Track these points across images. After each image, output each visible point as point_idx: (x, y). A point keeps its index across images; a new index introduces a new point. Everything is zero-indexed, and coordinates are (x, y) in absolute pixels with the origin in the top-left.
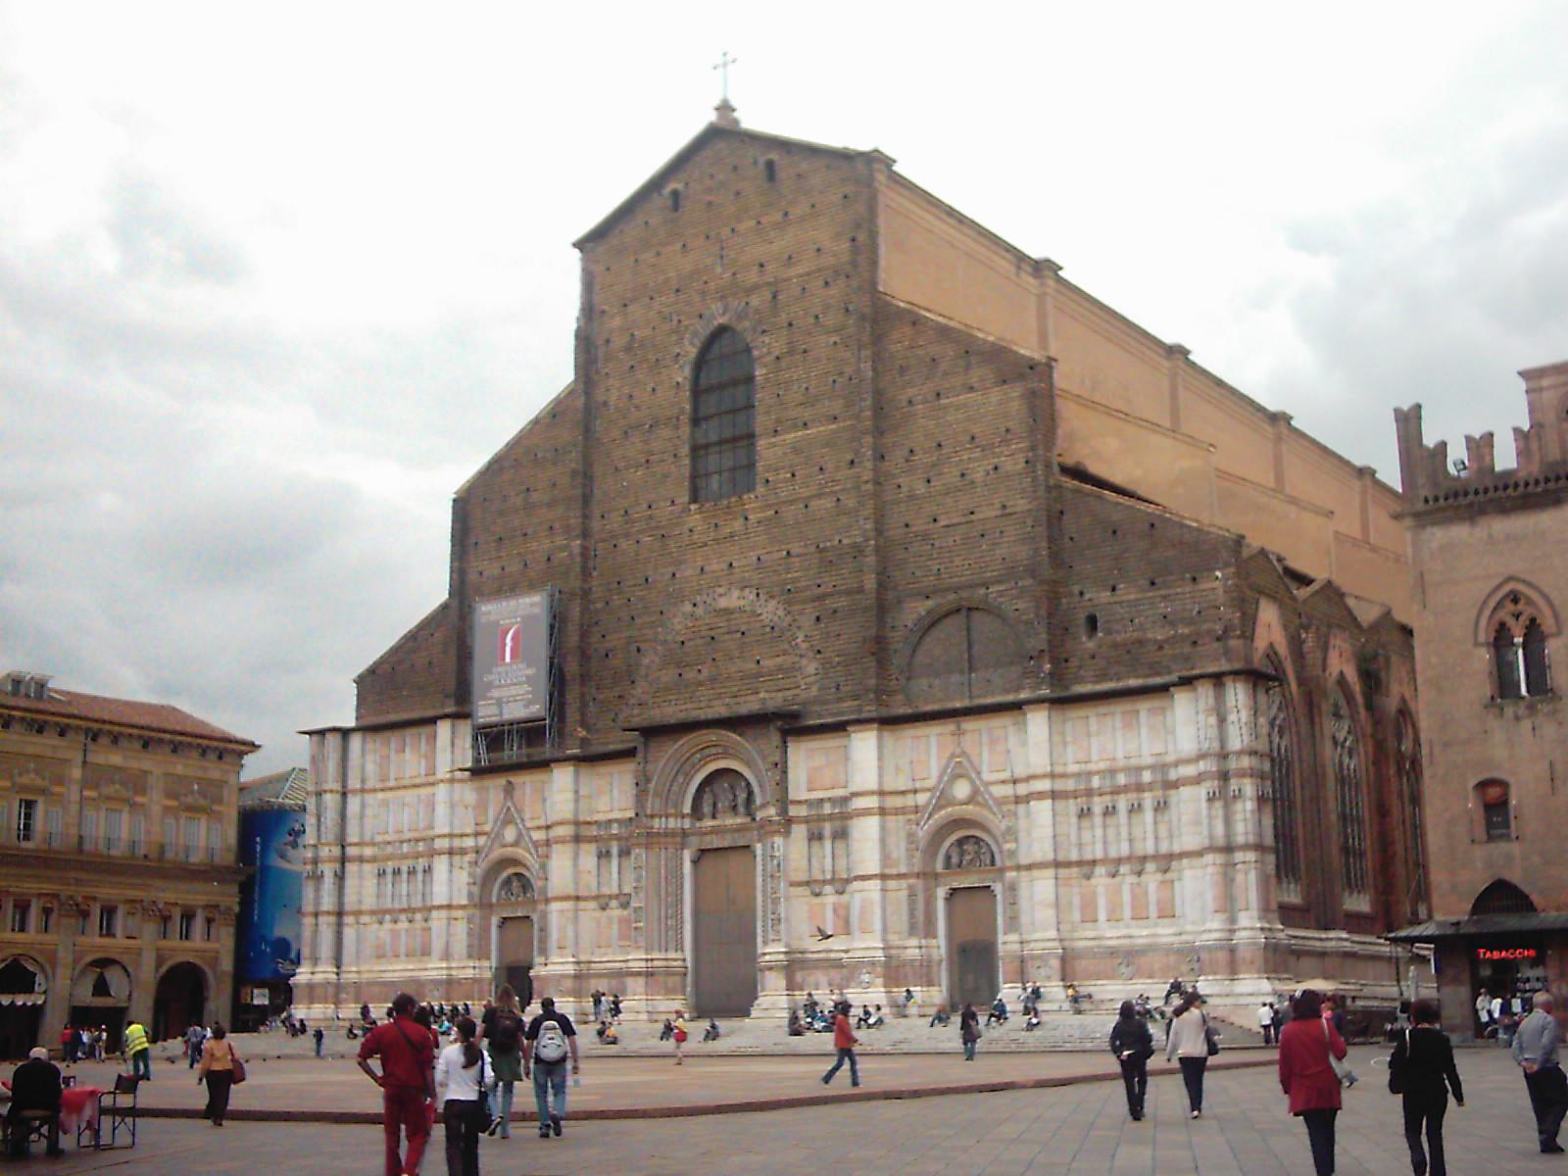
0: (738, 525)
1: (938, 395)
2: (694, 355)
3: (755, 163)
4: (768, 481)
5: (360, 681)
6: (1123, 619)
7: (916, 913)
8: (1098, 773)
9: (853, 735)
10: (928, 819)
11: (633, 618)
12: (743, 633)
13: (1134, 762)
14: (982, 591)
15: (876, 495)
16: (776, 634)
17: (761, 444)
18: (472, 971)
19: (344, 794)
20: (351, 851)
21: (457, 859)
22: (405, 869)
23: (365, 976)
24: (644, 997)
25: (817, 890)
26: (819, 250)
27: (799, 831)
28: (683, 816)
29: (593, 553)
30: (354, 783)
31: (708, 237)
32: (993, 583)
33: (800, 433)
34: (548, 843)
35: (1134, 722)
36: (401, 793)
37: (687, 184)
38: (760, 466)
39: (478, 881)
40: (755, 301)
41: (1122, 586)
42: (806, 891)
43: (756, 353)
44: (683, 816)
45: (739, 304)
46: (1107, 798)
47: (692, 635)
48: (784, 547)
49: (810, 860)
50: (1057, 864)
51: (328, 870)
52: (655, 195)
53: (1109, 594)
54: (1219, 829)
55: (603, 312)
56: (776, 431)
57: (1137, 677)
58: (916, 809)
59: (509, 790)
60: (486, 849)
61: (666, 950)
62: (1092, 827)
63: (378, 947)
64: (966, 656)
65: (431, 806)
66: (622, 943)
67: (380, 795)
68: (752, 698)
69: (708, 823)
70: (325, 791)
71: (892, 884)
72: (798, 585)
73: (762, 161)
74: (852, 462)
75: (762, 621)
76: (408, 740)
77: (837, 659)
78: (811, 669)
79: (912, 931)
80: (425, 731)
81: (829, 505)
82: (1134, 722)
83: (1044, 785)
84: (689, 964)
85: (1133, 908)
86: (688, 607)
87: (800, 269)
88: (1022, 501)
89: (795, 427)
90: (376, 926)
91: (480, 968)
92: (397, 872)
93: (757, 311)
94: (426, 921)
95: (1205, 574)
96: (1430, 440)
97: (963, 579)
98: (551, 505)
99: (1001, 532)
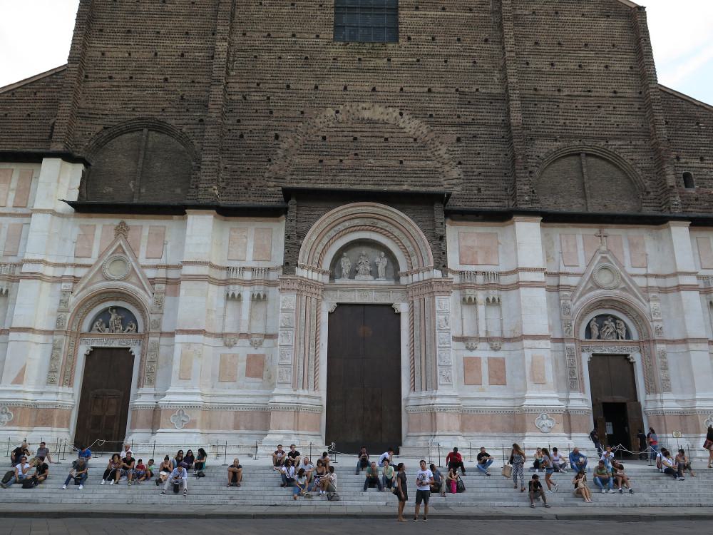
1: (557, 13)
4: (409, 38)
7: (576, 371)
9: (516, 223)
10: (579, 298)
11: (271, 113)
12: (386, 139)
14: (603, 143)
17: (403, 13)
24: (293, 432)
25: (474, 346)
27: (455, 296)
32: (610, 138)
33: (440, 13)
34: (177, 282)
38: (402, 27)
39: (72, 310)
41: (707, 158)
42: (461, 345)
44: (324, 273)
47: (335, 134)
48: (426, 85)
49: (462, 319)
53: (698, 161)
58: (568, 288)
59: (122, 230)
60: (86, 281)
61: (308, 388)
65: (17, 237)
72: (440, 113)
74: (486, 40)
77: (478, 170)
78: (456, 172)
80: (17, 169)
83: (691, 280)
84: (324, 403)
86: (330, 112)
88: (628, 91)
89: (436, 9)
91: (62, 393)
97: (586, 132)
98: (189, 16)
99: (614, 108)
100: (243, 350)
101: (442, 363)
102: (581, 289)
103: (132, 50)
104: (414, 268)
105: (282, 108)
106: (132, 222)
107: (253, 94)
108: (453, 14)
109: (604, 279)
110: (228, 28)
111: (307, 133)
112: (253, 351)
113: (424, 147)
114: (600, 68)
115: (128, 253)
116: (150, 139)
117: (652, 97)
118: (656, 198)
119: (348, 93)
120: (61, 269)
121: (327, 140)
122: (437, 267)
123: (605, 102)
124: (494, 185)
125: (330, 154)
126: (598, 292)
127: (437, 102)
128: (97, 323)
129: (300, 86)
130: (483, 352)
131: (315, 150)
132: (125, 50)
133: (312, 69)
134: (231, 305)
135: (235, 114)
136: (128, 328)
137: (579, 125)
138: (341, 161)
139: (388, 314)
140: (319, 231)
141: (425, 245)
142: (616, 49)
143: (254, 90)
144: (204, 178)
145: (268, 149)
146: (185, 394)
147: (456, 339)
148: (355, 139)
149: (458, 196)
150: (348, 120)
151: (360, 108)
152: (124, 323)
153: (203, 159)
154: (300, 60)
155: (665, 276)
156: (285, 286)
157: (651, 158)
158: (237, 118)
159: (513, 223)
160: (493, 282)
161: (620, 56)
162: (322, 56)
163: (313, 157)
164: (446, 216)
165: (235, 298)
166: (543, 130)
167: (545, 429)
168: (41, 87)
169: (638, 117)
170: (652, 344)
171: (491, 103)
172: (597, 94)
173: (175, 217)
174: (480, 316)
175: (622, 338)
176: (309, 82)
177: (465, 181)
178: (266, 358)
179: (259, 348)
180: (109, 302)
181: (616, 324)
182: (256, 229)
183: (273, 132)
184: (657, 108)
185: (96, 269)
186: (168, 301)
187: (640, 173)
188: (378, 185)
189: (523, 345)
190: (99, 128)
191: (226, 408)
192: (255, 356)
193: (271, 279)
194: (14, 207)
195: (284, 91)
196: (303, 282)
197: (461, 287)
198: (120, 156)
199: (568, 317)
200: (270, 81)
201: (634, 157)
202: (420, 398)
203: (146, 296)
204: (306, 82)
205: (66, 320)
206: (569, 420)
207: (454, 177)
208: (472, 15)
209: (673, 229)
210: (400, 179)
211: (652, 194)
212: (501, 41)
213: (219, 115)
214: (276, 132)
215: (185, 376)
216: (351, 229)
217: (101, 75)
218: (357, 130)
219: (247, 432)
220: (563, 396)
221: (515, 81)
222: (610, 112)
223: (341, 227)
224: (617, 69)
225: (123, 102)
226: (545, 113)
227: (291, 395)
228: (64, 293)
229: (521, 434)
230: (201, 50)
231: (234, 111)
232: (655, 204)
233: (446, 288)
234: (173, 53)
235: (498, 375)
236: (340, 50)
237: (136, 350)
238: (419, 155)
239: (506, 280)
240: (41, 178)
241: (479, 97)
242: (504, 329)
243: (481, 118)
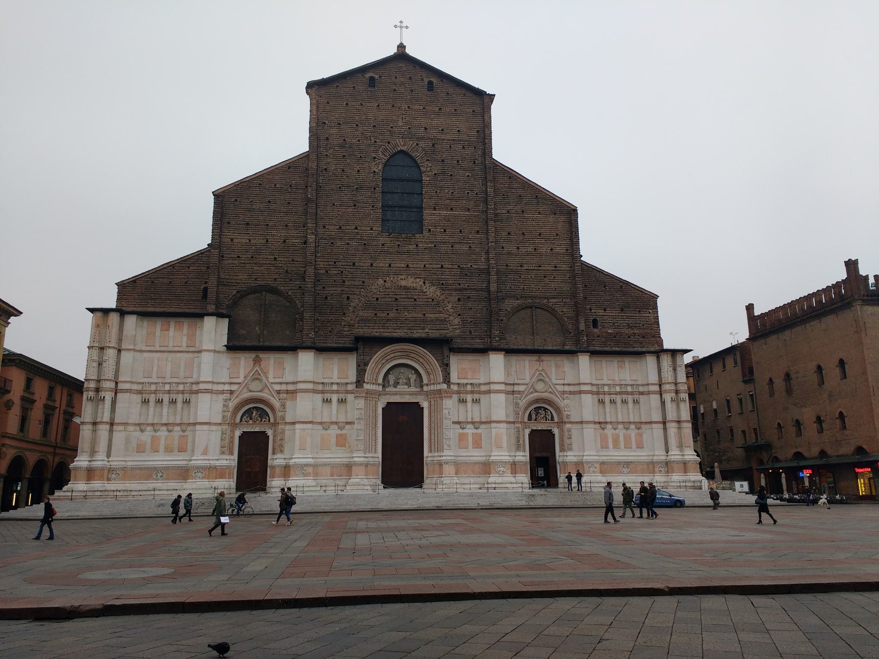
0: (412, 247)
1: (523, 212)
2: (383, 160)
3: (422, 79)
4: (430, 230)
5: (121, 285)
6: (610, 323)
7: (521, 440)
8: (607, 385)
10: (525, 397)
11: (344, 282)
12: (415, 300)
13: (623, 382)
14: (546, 301)
15: (495, 249)
16: (435, 304)
17: (426, 212)
18: (225, 462)
19: (119, 351)
20: (121, 386)
21: (214, 396)
22: (166, 398)
23: (129, 463)
26: (459, 131)
28: (379, 385)
29: (317, 245)
30: (124, 346)
31: (393, 106)
34: (294, 392)
35: (623, 366)
36: (165, 355)
37: (380, 77)
38: (425, 223)
39: (231, 410)
40: (422, 144)
41: (608, 309)
42: (458, 426)
43: (422, 169)
44: (379, 385)
45: (412, 145)
46: (614, 396)
50: (595, 423)
51: (108, 396)
52: (360, 75)
53: (603, 311)
54: (675, 414)
55: (325, 123)
56: (435, 208)
57: (618, 347)
58: (519, 392)
59: (257, 361)
62: (604, 408)
63: (139, 446)
64: (535, 328)
66: (339, 448)
67: (146, 355)
68: (421, 331)
69: (390, 389)
70: (109, 347)
71: (509, 426)
72: (448, 282)
73: (426, 80)
74: (478, 232)
75: (426, 295)
76: (172, 324)
79: (519, 447)
81: (466, 249)
82: (623, 366)
85: (625, 444)
86: (381, 281)
87: (448, 137)
88: (565, 266)
90: (138, 433)
92: (160, 402)
93: (423, 150)
94: (184, 431)
95: (645, 310)
96: (863, 272)
97: (537, 294)
99: (554, 277)
100: (334, 431)
101: (446, 438)
102: (526, 392)
103: (251, 237)
104: (432, 382)
105: (351, 279)
106: (262, 355)
107: (332, 269)
108: (458, 213)
109: (540, 386)
110: (315, 225)
111: (367, 296)
112: (339, 432)
113: (438, 304)
114: (548, 251)
115: (262, 375)
116: (267, 298)
117: (576, 272)
118: (574, 336)
119: (392, 269)
120: (222, 385)
121: (379, 300)
122: (444, 382)
123: (549, 274)
124: (477, 329)
125: (381, 309)
126: (536, 394)
127: (446, 275)
128: (245, 417)
129: (362, 264)
130: (470, 430)
131: (372, 307)
132: (246, 238)
133: (368, 252)
134: (326, 405)
135: (321, 283)
136: (264, 420)
137: (532, 289)
138: (388, 314)
139: (416, 409)
140: (376, 360)
141: (437, 369)
142: (558, 237)
143: (332, 266)
144: (305, 327)
145: (343, 307)
146: (303, 458)
147: (454, 423)
148: (396, 299)
149: (458, 336)
150: (392, 287)
151: (399, 279)
152: (261, 417)
153: (304, 316)
154: (361, 246)
155: (574, 385)
156: (358, 395)
157: (574, 311)
158: (323, 286)
159: (489, 355)
160: (476, 390)
161: (560, 242)
162: (375, 243)
163: (371, 311)
164: (450, 351)
165: (328, 401)
166: (510, 293)
167: (501, 472)
168: (192, 262)
169: (568, 283)
170: (564, 424)
171: (480, 275)
172: (545, 268)
173: (289, 352)
174: (468, 410)
175: (549, 420)
176: (367, 261)
177: (463, 326)
178: (347, 436)
179: (343, 430)
180: (251, 405)
181: (545, 412)
182: (339, 358)
183: (345, 295)
184: (579, 279)
185: (244, 385)
186: (288, 404)
187: (566, 320)
188: (411, 329)
189: (491, 426)
190: (234, 292)
191: (325, 465)
192: (341, 435)
193: (348, 389)
194: (187, 346)
195: (351, 267)
196: (368, 392)
197: (458, 392)
198: (248, 309)
199: (518, 409)
200: (342, 261)
201: (563, 310)
202: (434, 457)
203: (275, 401)
204: (364, 261)
205: (228, 416)
206: (514, 467)
207: (456, 324)
208: (469, 213)
209: (580, 357)
210: (423, 325)
211: (572, 333)
212: (487, 233)
213: (313, 286)
214: (348, 295)
215: (302, 449)
216: (395, 358)
217: (231, 256)
218: (398, 293)
219: (338, 478)
220: (513, 454)
221: (494, 262)
222: (552, 280)
223: (389, 357)
224: (558, 251)
225: (249, 274)
226: (512, 281)
227: (363, 457)
228: (225, 400)
229: (489, 476)
230: (297, 237)
231: (322, 281)
232: (573, 340)
233: (449, 394)
234: (278, 240)
235: (477, 444)
236: (386, 239)
237: (270, 433)
238: (435, 310)
239: (483, 388)
240: (205, 329)
241: (473, 271)
242: (482, 416)
243: (473, 285)
